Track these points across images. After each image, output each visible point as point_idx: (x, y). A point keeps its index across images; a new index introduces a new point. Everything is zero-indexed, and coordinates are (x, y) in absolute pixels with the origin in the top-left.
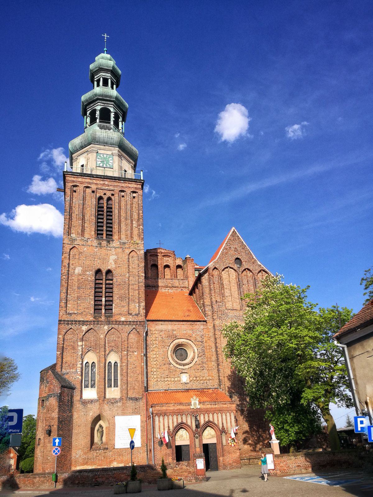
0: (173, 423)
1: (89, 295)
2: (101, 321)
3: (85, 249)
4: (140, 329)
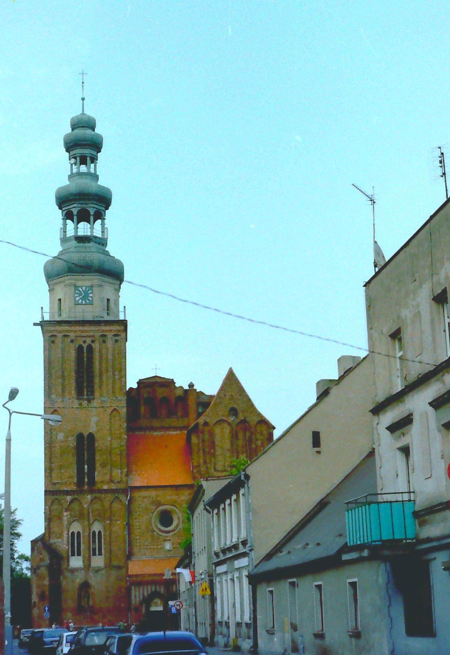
0: (147, 592)
1: (72, 463)
2: (85, 491)
3: (66, 412)
4: (122, 497)
